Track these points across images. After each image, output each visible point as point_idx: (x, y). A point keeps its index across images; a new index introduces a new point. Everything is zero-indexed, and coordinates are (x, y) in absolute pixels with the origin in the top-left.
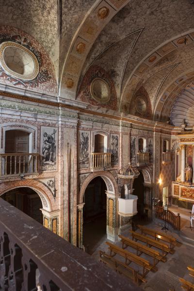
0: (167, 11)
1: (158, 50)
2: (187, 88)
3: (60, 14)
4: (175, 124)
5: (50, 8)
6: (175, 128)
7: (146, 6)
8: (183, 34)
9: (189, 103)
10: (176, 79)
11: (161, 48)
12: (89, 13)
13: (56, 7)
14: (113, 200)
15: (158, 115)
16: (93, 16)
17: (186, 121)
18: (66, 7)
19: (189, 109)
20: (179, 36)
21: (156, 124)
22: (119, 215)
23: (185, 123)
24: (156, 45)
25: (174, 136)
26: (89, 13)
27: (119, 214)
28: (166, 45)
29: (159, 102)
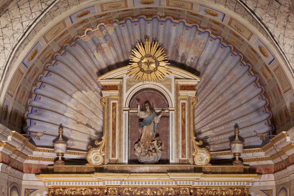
2: (85, 38)
6: (36, 154)
9: (77, 80)
10: (73, 9)
15: (7, 109)
17: (66, 132)
19: (75, 96)
21: (10, 138)
23: (65, 139)
25: (32, 176)
29: (19, 70)
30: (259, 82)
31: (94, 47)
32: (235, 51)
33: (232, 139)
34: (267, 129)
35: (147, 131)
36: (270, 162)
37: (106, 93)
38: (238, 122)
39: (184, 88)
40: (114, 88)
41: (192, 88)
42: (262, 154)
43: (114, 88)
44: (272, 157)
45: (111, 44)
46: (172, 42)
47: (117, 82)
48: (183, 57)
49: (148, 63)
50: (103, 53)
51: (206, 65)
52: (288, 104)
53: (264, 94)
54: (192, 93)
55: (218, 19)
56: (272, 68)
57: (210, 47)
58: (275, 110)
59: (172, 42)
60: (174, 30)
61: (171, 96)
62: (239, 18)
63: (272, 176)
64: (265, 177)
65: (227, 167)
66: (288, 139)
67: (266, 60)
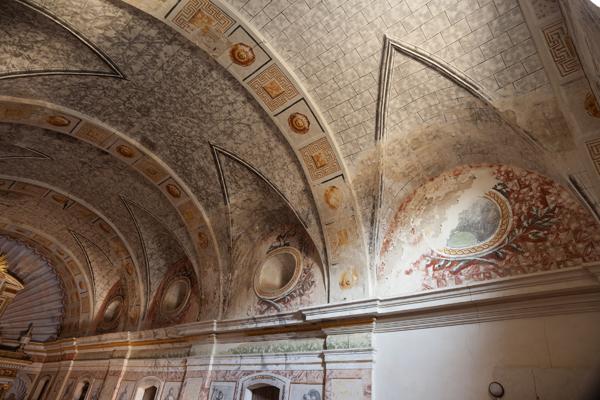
0: (95, 176)
1: (20, 182)
3: (29, 74)
5: (28, 58)
7: (91, 157)
8: (71, 196)
11: (27, 184)
12: (49, 105)
13: (37, 67)
16: (46, 111)
18: (45, 80)
20: (65, 193)
24: (26, 176)
26: (49, 105)
28: (40, 187)
30: (64, 300)
32: (58, 277)
33: (24, 333)
34: (54, 331)
36: (45, 355)
38: (34, 322)
41: (14, 292)
42: (42, 348)
44: (48, 352)
46: (16, 259)
48: (18, 270)
51: (34, 279)
52: (81, 321)
53: (64, 309)
54: (12, 295)
56: (80, 296)
57: (42, 269)
58: (66, 322)
59: (16, 259)
60: (24, 252)
62: (77, 261)
63: (41, 365)
64: (35, 364)
65: (10, 353)
66: (75, 343)
67: (80, 291)
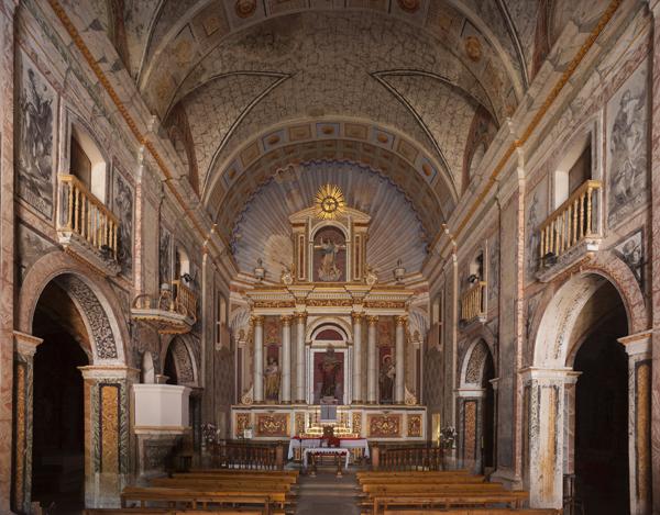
2: (278, 179)
4: (241, 265)
14: (118, 386)
22: (136, 435)
27: (137, 432)
31: (285, 194)
35: (328, 258)
37: (295, 230)
39: (359, 225)
40: (302, 225)
43: (302, 225)
45: (300, 193)
47: (304, 221)
49: (329, 204)
50: (293, 200)
54: (364, 229)
55: (387, 147)
61: (348, 232)
